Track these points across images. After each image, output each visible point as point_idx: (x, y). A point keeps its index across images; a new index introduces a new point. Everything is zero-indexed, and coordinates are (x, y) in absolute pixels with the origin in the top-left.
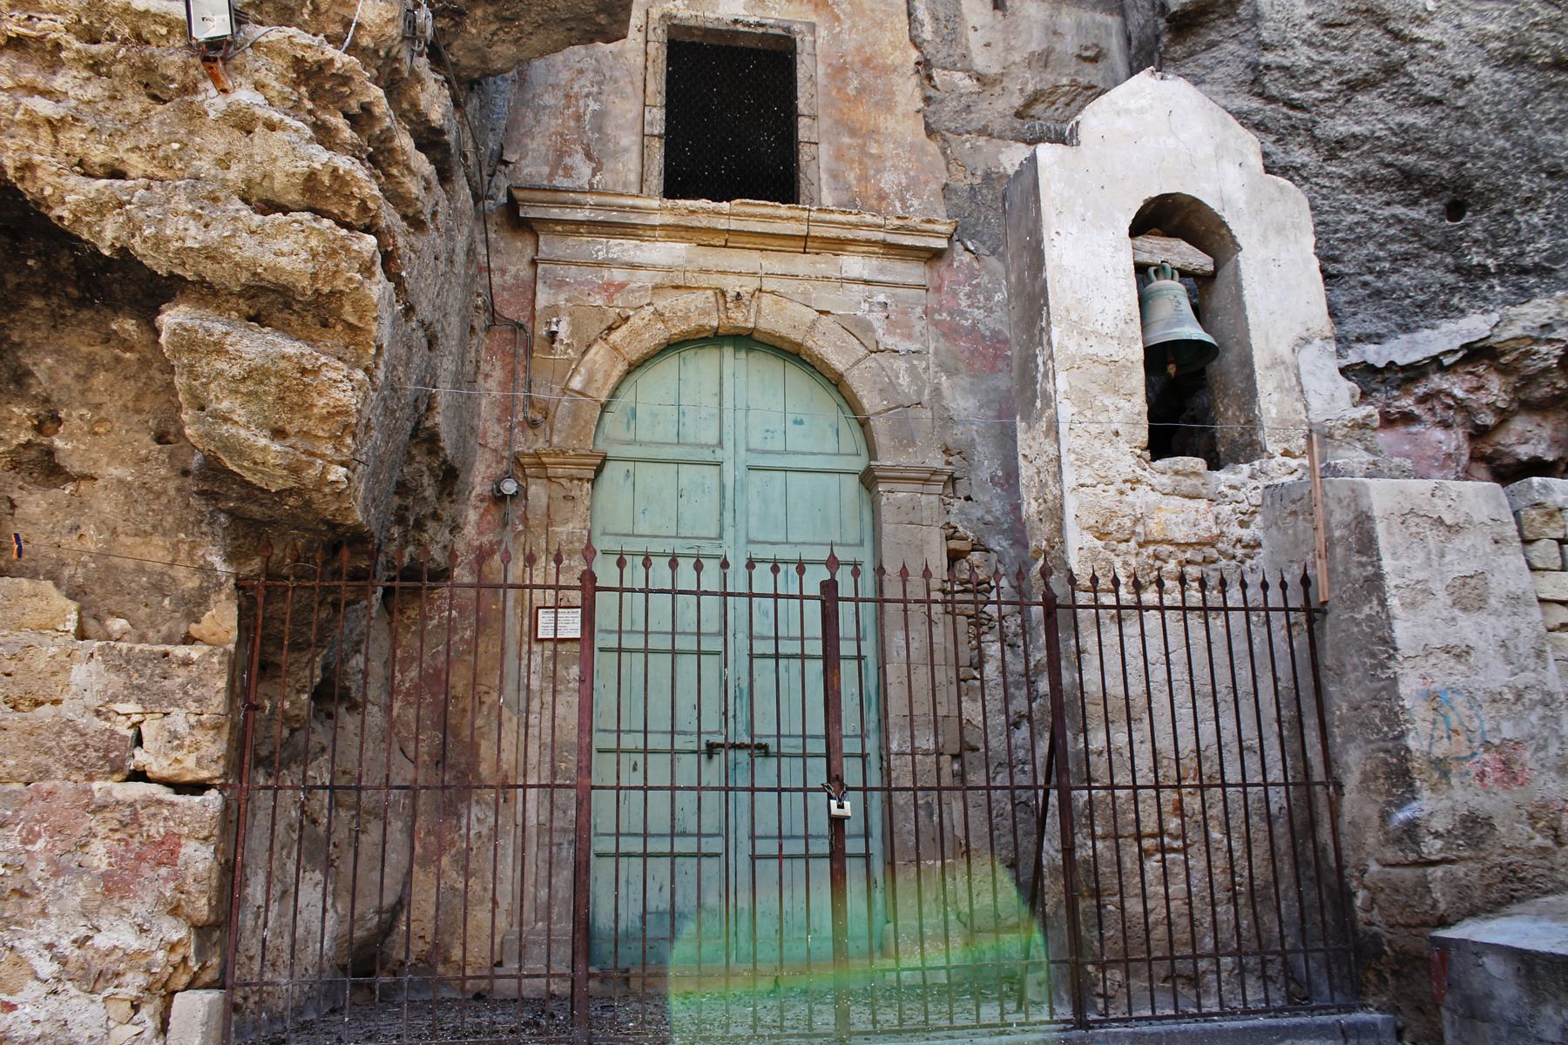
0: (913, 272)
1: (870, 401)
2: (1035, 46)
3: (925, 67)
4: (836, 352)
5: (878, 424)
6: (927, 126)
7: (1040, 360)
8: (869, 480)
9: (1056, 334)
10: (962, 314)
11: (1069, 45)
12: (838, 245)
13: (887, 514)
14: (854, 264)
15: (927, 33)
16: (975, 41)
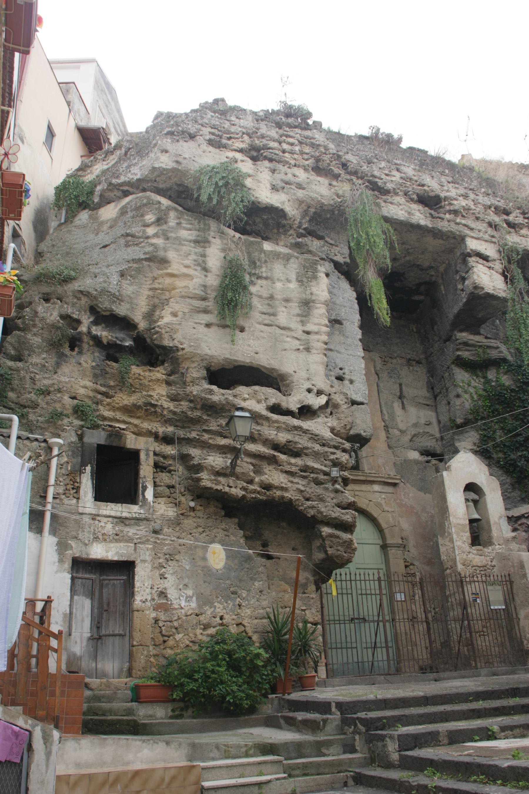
0: (390, 489)
1: (384, 525)
2: (414, 421)
3: (386, 427)
4: (375, 512)
5: (386, 531)
6: (388, 445)
7: (446, 524)
8: (384, 547)
9: (451, 518)
10: (403, 500)
11: (422, 421)
12: (372, 482)
13: (391, 556)
14: (376, 487)
15: (386, 417)
16: (399, 420)
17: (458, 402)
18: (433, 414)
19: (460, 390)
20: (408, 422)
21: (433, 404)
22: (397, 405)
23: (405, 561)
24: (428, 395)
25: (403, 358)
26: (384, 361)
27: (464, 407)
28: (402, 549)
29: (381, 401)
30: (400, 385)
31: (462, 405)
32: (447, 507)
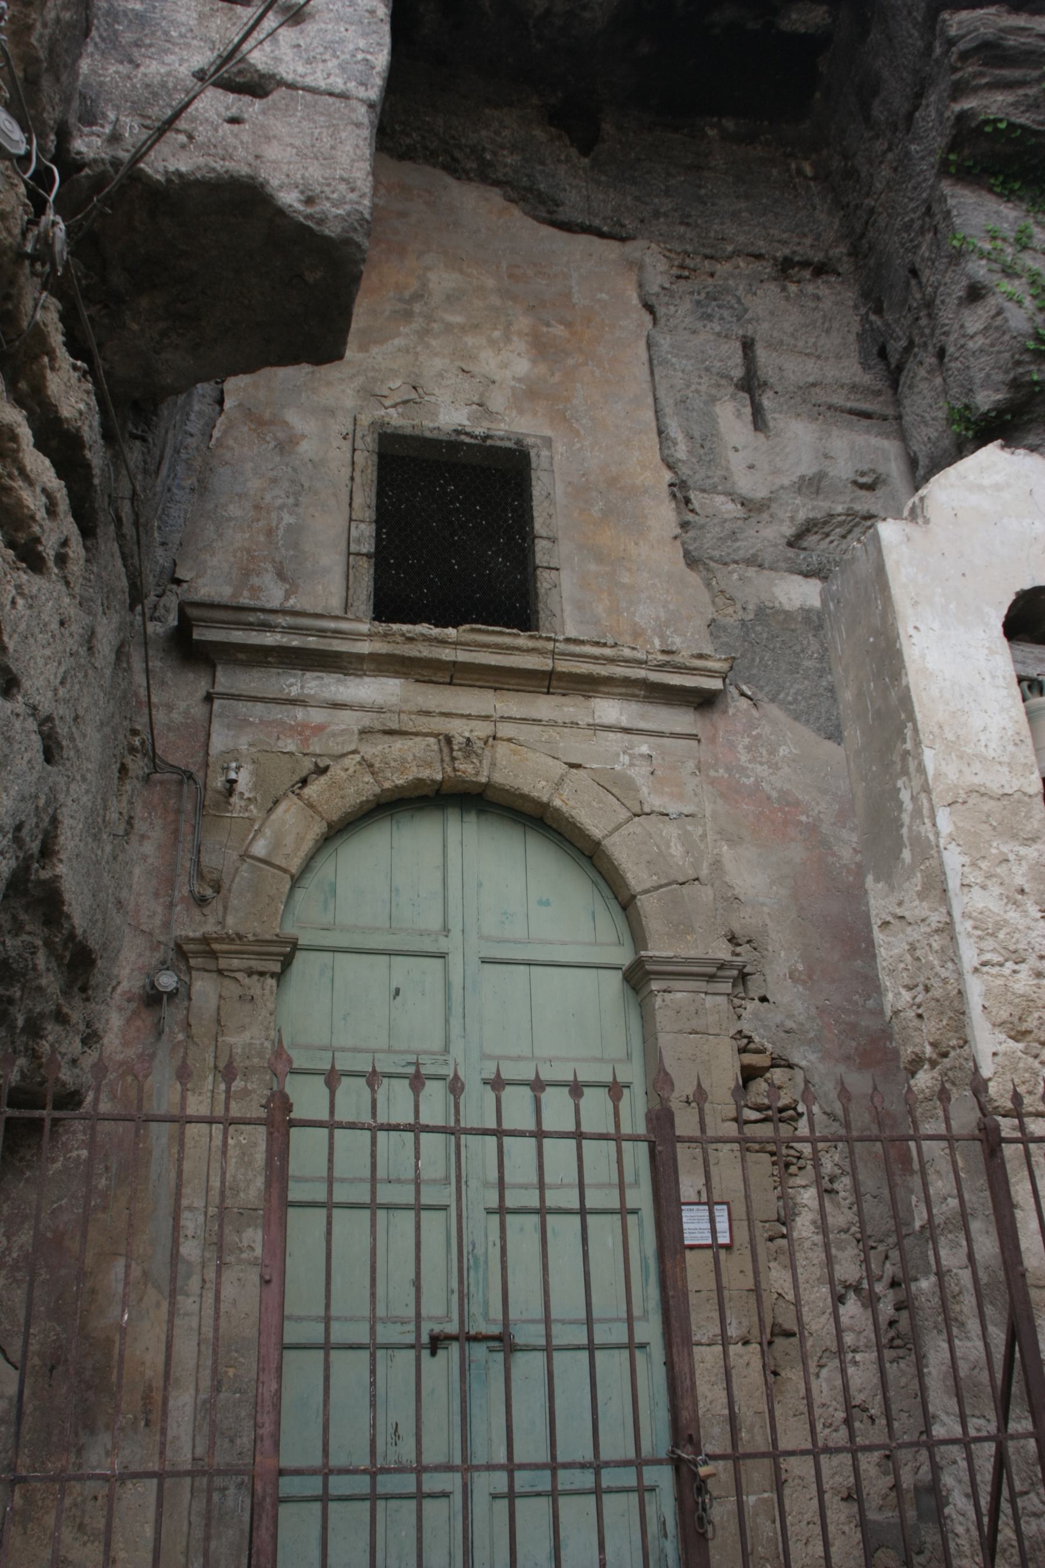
0: (682, 720)
1: (637, 876)
2: (807, 468)
3: (680, 492)
4: (593, 817)
5: (647, 904)
6: (687, 554)
7: (905, 796)
8: (638, 977)
9: (929, 757)
10: (743, 770)
11: (843, 469)
12: (589, 685)
13: (663, 1019)
14: (610, 710)
15: (681, 451)
16: (737, 462)
17: (975, 320)
18: (891, 447)
19: (979, 269)
20: (776, 472)
21: (890, 411)
22: (731, 418)
23: (745, 1045)
24: (866, 379)
25: (759, 257)
26: (682, 267)
27: (1002, 330)
28: (727, 987)
29: (661, 393)
30: (748, 346)
31: (996, 326)
32: (906, 701)
